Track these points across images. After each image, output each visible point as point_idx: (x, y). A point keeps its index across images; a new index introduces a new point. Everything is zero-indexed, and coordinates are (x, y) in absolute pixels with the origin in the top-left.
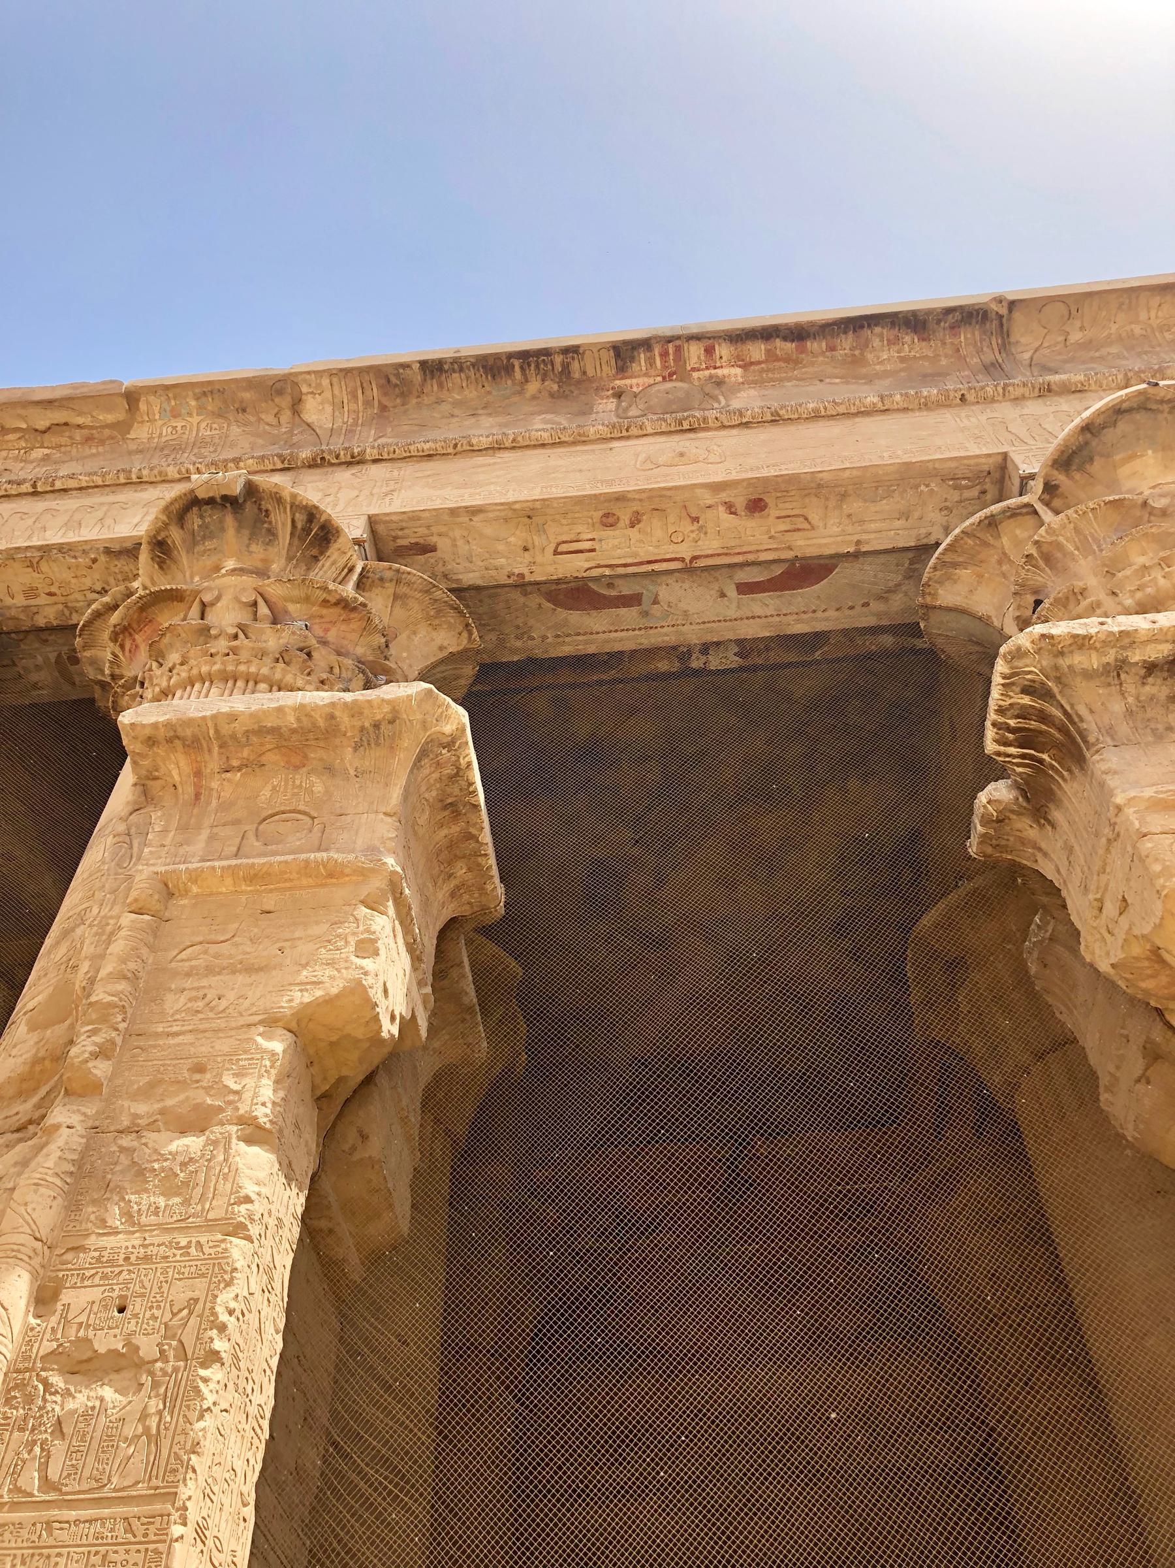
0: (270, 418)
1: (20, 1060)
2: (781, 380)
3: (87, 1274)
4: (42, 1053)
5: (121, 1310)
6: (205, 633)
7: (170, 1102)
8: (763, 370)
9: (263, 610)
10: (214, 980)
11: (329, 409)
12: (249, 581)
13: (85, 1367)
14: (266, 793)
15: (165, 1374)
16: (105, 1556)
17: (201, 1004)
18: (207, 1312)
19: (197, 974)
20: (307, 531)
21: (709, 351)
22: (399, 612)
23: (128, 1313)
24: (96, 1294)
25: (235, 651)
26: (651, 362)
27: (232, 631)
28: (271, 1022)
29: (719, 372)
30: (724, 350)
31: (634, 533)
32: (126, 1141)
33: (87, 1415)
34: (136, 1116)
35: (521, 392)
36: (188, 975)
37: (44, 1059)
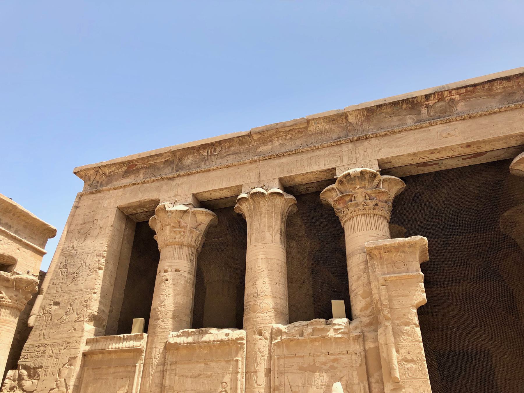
0: (340, 122)
2: (470, 98)
6: (357, 205)
7: (402, 321)
8: (464, 95)
9: (367, 197)
10: (399, 298)
11: (354, 118)
12: (362, 190)
14: (393, 257)
20: (372, 176)
21: (450, 92)
22: (390, 185)
24: (404, 351)
25: (364, 209)
26: (435, 97)
27: (363, 203)
28: (412, 306)
29: (453, 97)
30: (454, 92)
31: (438, 154)
32: (398, 327)
35: (402, 108)
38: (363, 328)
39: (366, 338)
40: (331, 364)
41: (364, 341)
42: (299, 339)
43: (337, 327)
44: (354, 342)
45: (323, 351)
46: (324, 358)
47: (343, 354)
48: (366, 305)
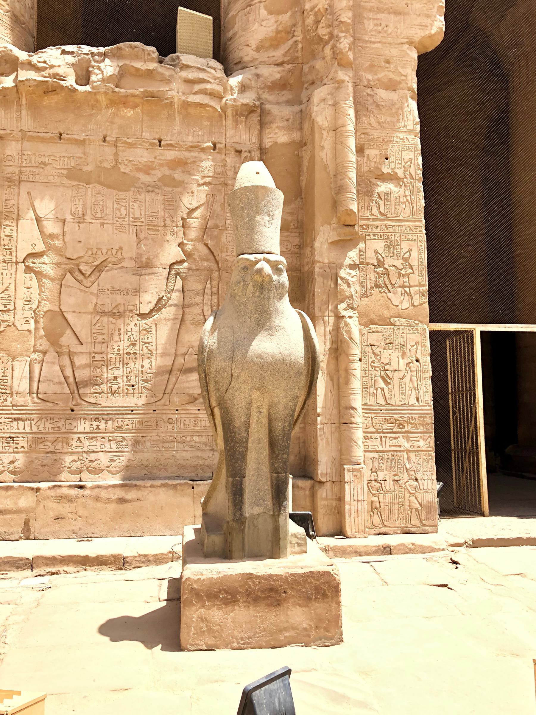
1: (270, 29)
3: (373, 144)
4: (280, 28)
5: (387, 159)
13: (380, 177)
15: (408, 183)
16: (406, 236)
17: (380, 28)
18: (416, 164)
19: (374, 11)
23: (390, 159)
28: (410, 43)
32: (369, 91)
33: (387, 193)
34: (369, 80)
36: (370, 11)
37: (282, 31)
38: (261, 92)
39: (268, 119)
40: (168, 172)
41: (262, 124)
42: (75, 90)
43: (191, 75)
44: (236, 122)
45: (146, 135)
46: (146, 153)
47: (203, 150)
48: (278, 32)
